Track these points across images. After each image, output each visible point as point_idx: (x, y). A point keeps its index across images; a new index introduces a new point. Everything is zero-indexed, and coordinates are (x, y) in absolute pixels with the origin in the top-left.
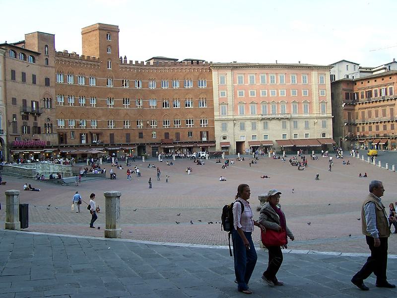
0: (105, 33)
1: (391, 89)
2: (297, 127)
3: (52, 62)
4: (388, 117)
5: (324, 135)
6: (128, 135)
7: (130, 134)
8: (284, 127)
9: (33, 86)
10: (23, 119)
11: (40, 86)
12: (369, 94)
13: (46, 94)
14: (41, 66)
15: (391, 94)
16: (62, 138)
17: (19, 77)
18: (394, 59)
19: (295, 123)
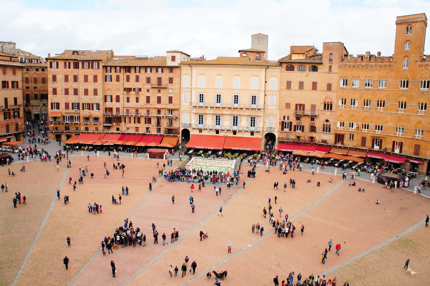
0: (404, 26)
3: (335, 68)
6: (417, 148)
7: (420, 145)
9: (314, 91)
10: (296, 120)
11: (322, 91)
13: (326, 98)
14: (324, 73)
16: (339, 137)
17: (295, 86)
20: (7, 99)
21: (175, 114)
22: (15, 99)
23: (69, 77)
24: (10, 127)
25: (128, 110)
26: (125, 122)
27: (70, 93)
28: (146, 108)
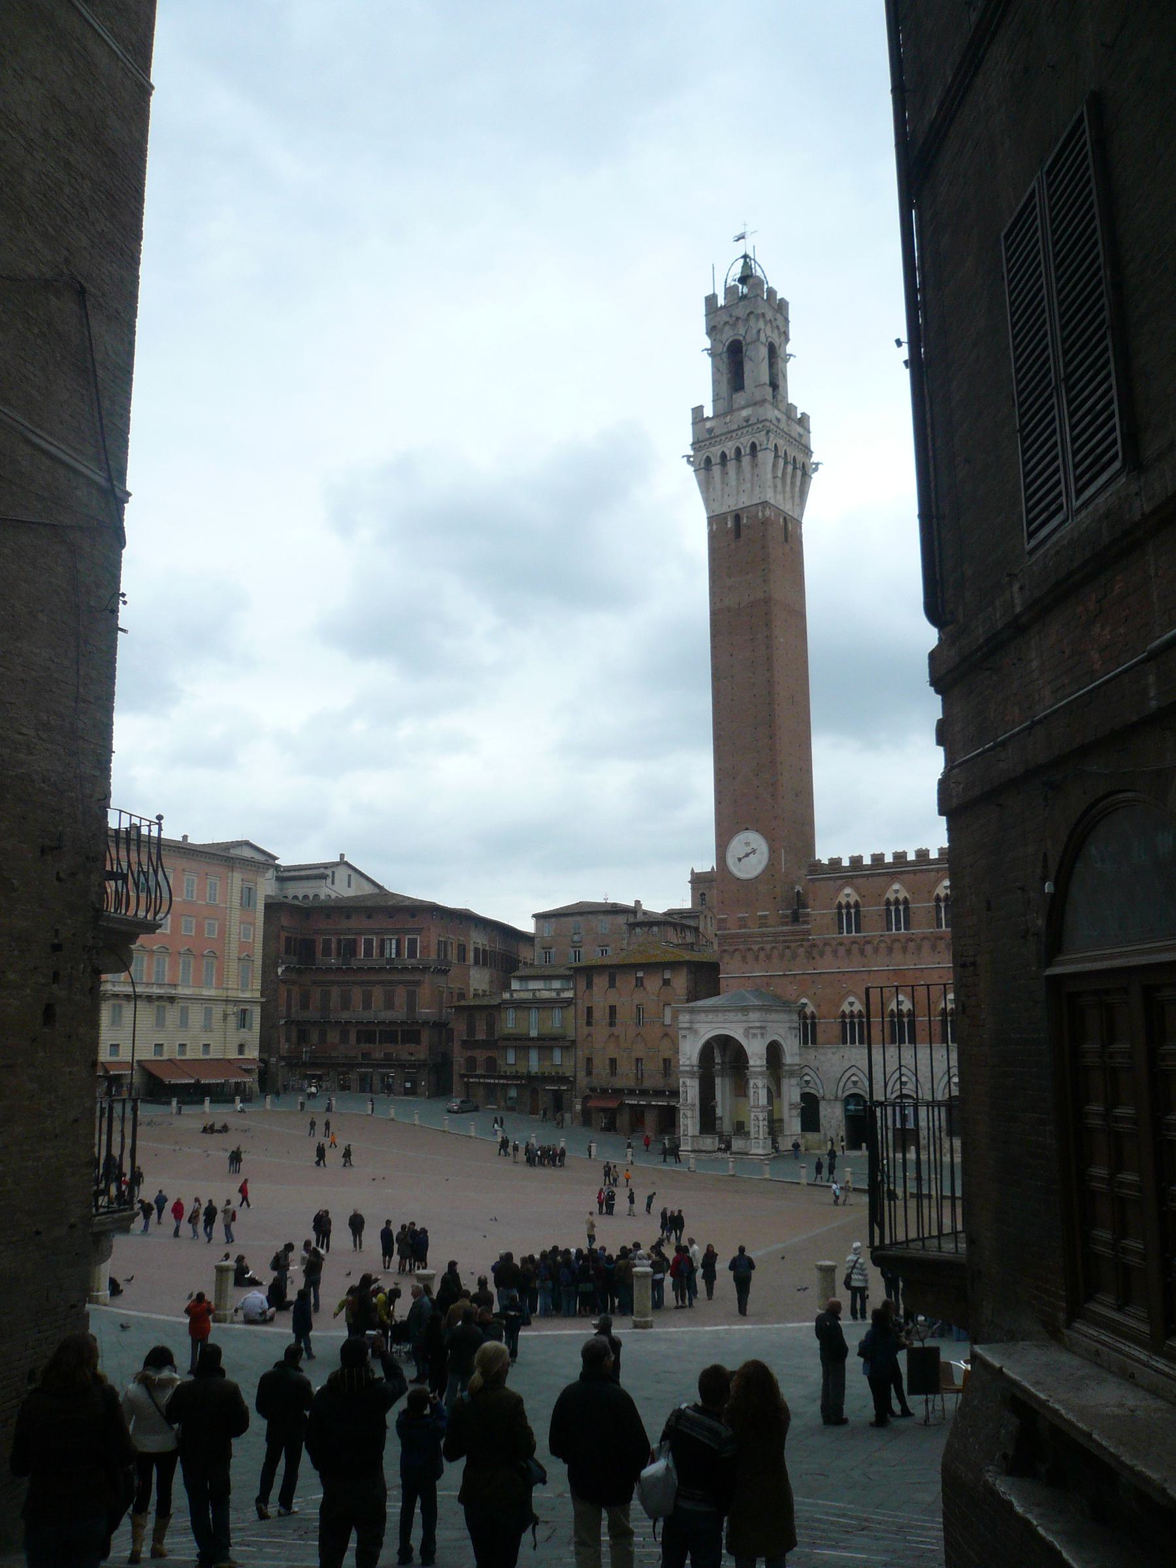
1: (413, 943)
2: (187, 1023)
4: (399, 1014)
5: (241, 1048)
8: (160, 1022)
12: (350, 949)
15: (412, 954)
18: (342, 856)
19: (184, 1012)
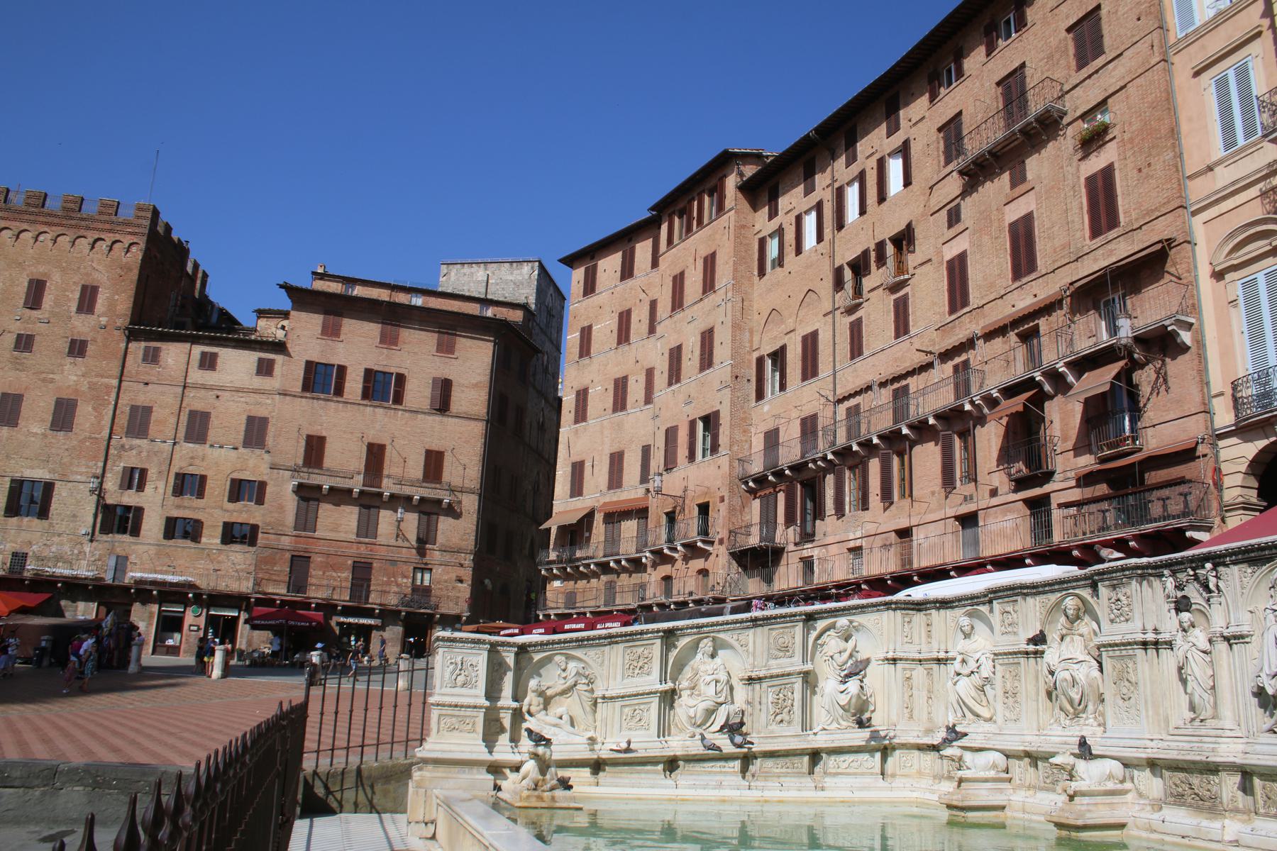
20: (382, 448)
21: (1149, 309)
22: (434, 462)
23: (634, 318)
24: (378, 579)
25: (854, 412)
26: (840, 511)
27: (630, 399)
28: (946, 356)
